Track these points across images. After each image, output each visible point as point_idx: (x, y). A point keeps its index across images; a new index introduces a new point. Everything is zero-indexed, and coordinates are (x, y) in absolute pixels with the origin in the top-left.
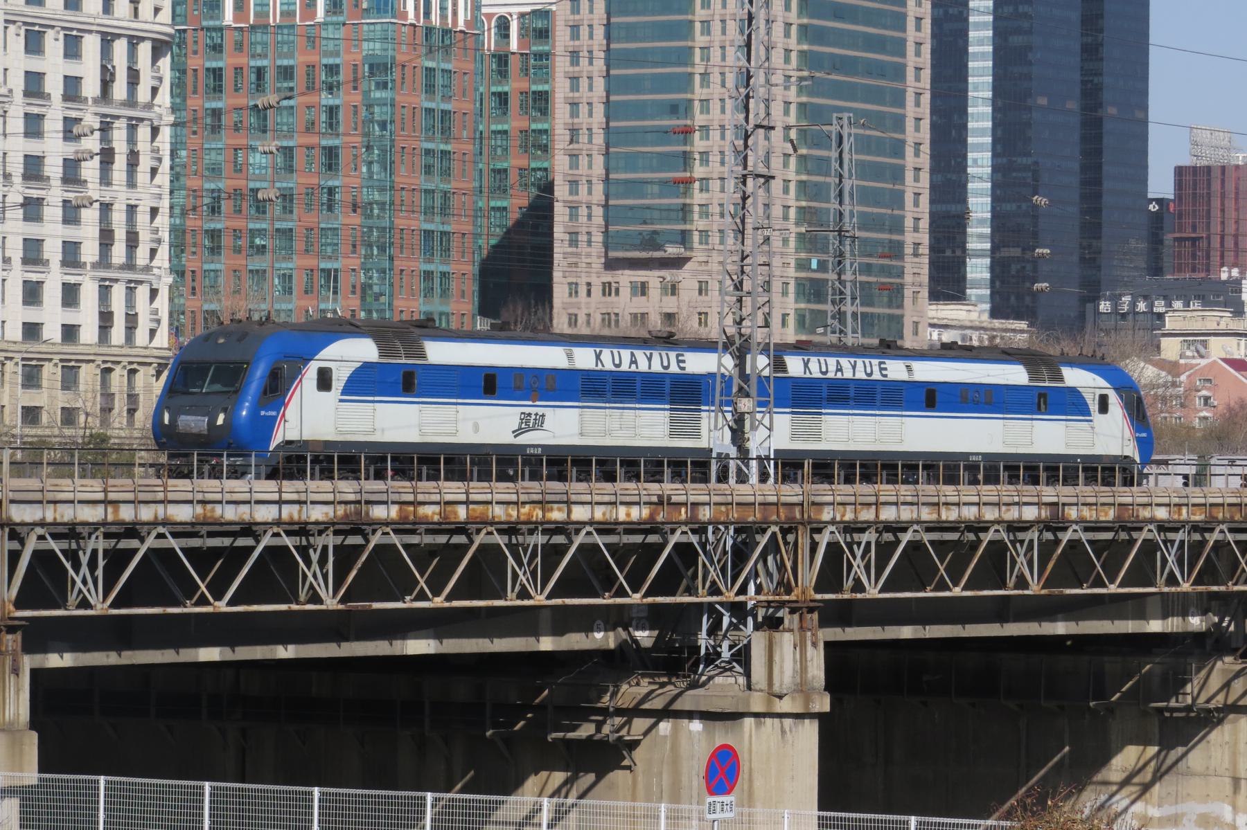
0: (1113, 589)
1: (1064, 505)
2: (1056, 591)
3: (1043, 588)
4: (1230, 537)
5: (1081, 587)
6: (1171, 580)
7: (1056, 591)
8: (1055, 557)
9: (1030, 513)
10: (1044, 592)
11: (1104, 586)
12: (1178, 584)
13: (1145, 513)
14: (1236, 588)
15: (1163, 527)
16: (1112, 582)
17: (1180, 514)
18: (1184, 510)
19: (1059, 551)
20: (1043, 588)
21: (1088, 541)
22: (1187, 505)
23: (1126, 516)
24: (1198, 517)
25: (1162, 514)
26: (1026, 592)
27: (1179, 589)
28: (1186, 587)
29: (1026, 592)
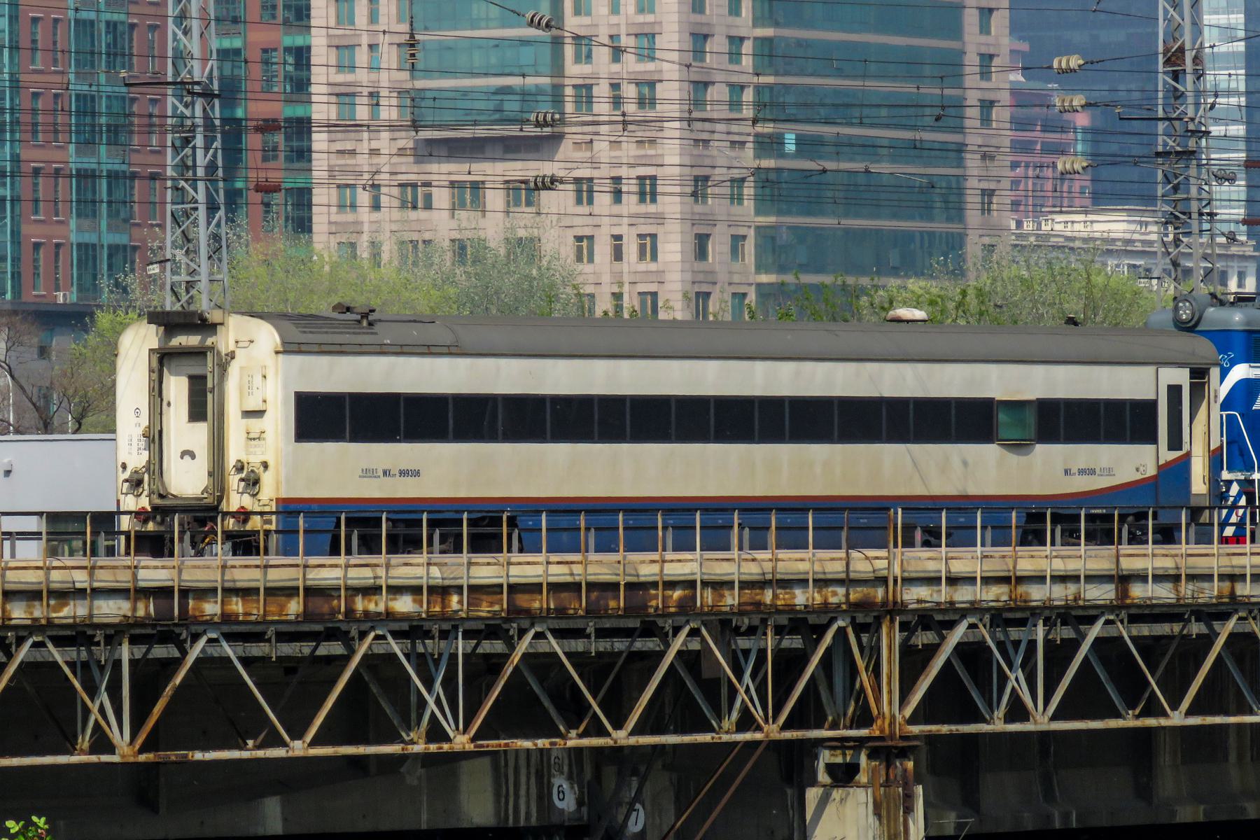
0: (298, 748)
1: (185, 593)
2: (173, 755)
3: (142, 750)
4: (555, 645)
5: (243, 747)
6: (435, 733)
7: (173, 755)
8: (169, 691)
9: (111, 610)
10: (142, 758)
11: (284, 744)
12: (448, 739)
13: (372, 607)
14: (570, 743)
15: (412, 630)
16: (297, 734)
17: (444, 605)
18: (455, 598)
19: (178, 680)
20: (142, 750)
21: (241, 659)
22: (459, 589)
23: (322, 606)
24: (484, 610)
25: (404, 605)
26: (105, 758)
27: (446, 747)
28: (461, 742)
29: (105, 758)
